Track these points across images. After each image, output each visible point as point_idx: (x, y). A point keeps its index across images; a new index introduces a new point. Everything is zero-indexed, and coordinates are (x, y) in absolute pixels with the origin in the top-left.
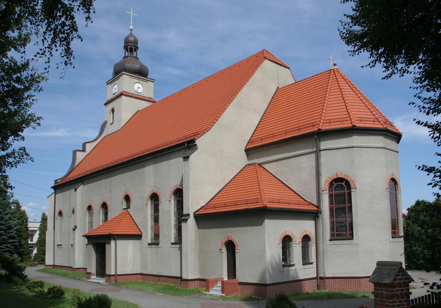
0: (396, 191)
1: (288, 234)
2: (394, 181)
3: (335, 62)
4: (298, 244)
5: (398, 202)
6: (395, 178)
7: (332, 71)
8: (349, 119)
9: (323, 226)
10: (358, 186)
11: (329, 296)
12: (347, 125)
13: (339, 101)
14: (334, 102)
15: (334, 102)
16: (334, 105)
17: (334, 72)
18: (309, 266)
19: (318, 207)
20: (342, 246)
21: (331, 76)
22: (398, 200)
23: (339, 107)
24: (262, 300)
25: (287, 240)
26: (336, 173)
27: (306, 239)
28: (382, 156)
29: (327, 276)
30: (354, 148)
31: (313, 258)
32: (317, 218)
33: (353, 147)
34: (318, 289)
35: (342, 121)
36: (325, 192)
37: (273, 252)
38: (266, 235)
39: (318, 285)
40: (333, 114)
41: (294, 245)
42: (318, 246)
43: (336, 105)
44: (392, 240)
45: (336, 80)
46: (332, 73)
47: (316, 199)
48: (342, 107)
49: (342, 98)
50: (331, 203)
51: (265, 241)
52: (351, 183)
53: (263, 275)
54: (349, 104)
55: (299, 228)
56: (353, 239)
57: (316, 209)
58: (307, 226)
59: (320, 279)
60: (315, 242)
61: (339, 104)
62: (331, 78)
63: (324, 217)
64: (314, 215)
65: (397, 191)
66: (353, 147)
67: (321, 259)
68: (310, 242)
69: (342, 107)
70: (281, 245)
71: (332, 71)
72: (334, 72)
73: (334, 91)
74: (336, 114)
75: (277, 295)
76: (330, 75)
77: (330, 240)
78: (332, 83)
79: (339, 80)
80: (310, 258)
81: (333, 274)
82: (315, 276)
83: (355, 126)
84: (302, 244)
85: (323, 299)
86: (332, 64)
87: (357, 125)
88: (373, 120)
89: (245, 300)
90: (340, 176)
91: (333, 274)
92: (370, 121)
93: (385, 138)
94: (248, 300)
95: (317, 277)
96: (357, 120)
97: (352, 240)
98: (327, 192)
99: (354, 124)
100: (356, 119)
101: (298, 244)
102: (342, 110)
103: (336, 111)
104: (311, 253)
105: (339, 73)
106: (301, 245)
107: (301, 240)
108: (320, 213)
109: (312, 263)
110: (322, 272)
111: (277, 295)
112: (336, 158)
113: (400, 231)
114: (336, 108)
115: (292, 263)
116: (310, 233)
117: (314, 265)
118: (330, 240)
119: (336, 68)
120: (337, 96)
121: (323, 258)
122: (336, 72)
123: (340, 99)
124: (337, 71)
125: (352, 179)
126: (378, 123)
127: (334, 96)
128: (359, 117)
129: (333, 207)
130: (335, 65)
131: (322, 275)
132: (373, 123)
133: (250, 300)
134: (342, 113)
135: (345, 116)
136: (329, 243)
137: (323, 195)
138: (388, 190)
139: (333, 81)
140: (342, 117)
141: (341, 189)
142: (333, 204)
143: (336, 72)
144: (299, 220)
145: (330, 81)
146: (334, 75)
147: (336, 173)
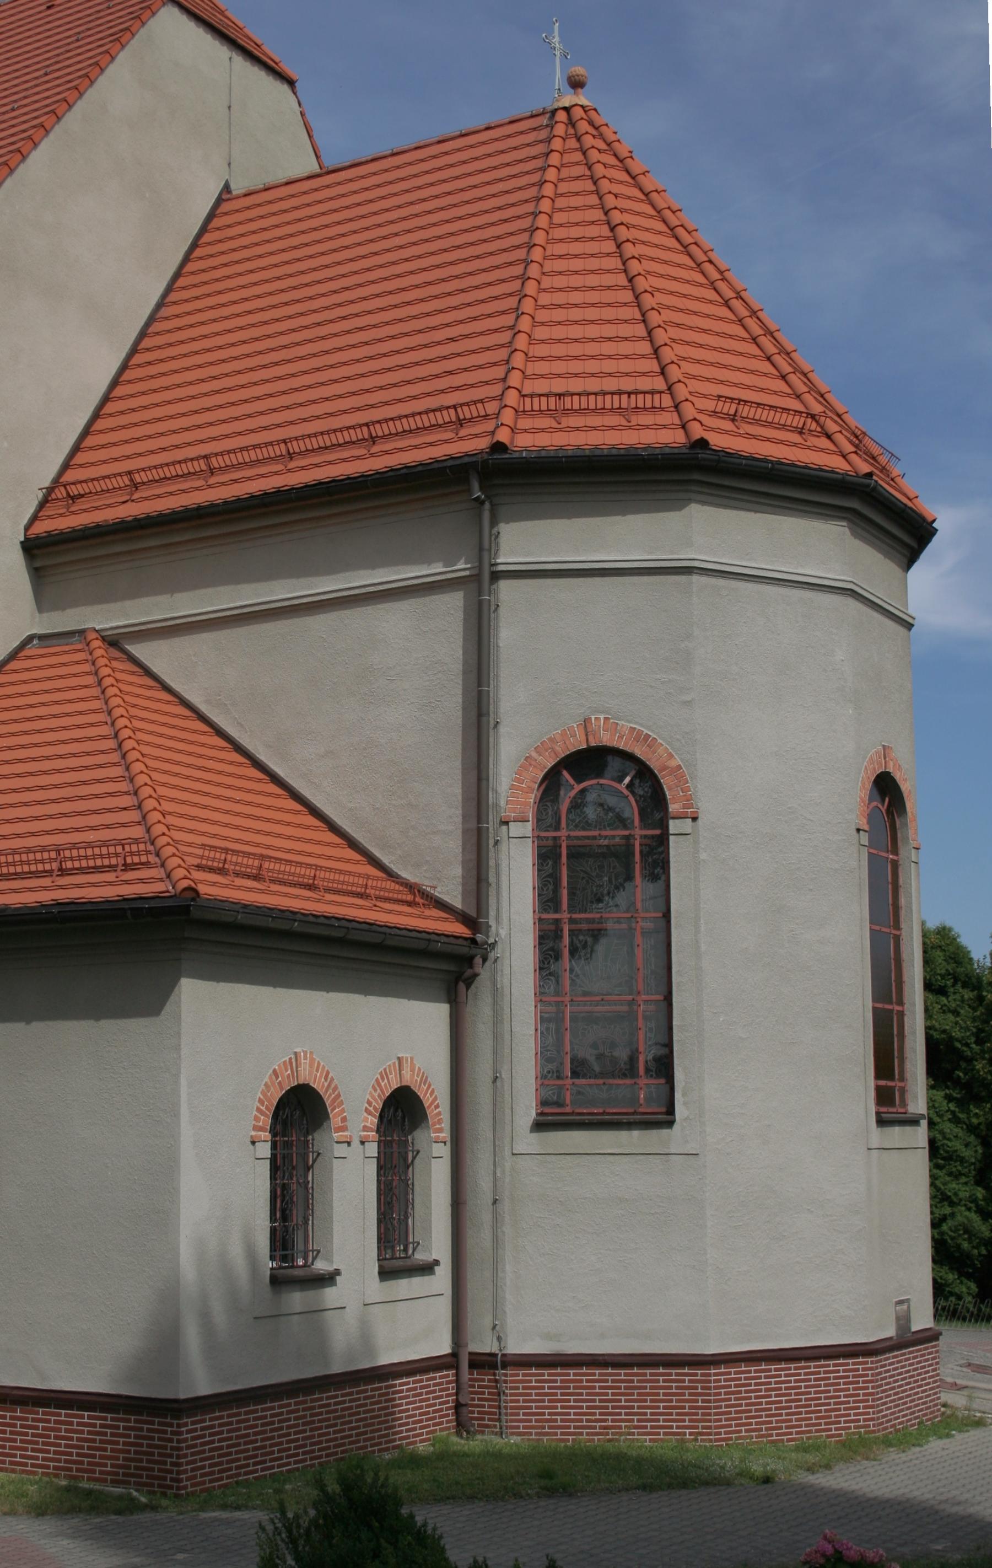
0: (895, 851)
1: (305, 1076)
2: (886, 788)
3: (579, 70)
4: (356, 1142)
5: (903, 913)
6: (897, 776)
7: (562, 116)
8: (667, 401)
9: (497, 1037)
10: (706, 805)
11: (547, 1474)
12: (661, 435)
13: (608, 296)
14: (576, 297)
15: (576, 297)
16: (576, 314)
17: (572, 123)
18: (415, 1285)
19: (473, 922)
20: (608, 1165)
21: (557, 144)
22: (903, 901)
23: (609, 330)
24: (153, 1508)
25: (299, 1113)
26: (587, 721)
27: (401, 1111)
28: (839, 637)
29: (515, 1347)
30: (695, 578)
31: (436, 1243)
32: (462, 986)
33: (688, 570)
34: (461, 1426)
35: (627, 404)
36: (516, 829)
37: (217, 1195)
38: (183, 1081)
39: (458, 1406)
40: (576, 367)
41: (340, 1150)
42: (468, 1157)
43: (592, 314)
44: (877, 1136)
45: (581, 170)
46: (560, 129)
47: (458, 871)
48: (625, 330)
49: (622, 280)
50: (547, 898)
51: (176, 1115)
52: (667, 782)
53: (164, 1344)
54: (667, 315)
55: (371, 1041)
56: (670, 1124)
57: (459, 929)
58: (398, 1036)
59: (475, 1368)
60: (446, 1135)
61: (609, 313)
62: (554, 159)
63: (503, 981)
64: (447, 964)
65: (902, 852)
66: (688, 570)
67: (479, 1239)
68: (420, 1138)
69: (625, 330)
70: (265, 1150)
71: (562, 116)
72: (572, 123)
73: (575, 232)
74: (592, 366)
75: (320, 1484)
76: (549, 140)
77: (540, 1126)
78: (563, 188)
79: (599, 170)
80: (416, 1234)
81: (548, 1337)
82: (443, 1347)
83: (702, 443)
84: (274, 1146)
85: (517, 1496)
86: (559, 79)
87: (717, 441)
88: (798, 421)
89: (40, 1511)
90: (606, 739)
91: (548, 1337)
92: (783, 427)
93: (855, 534)
94: (76, 1502)
95: (454, 1355)
96: (714, 414)
97: (665, 1132)
98: (527, 829)
99: (697, 432)
100: (710, 405)
101: (356, 1142)
102: (625, 348)
103: (592, 349)
104: (428, 1206)
105: (601, 136)
106: (372, 1149)
107: (373, 1121)
108: (485, 960)
109: (428, 1268)
110: (487, 1322)
111: (320, 1484)
112: (612, 629)
113: (910, 1086)
114: (593, 331)
115: (321, 1266)
116: (424, 1080)
117: (442, 1279)
118: (540, 1126)
119: (583, 101)
120: (593, 264)
121: (496, 1241)
122: (583, 126)
123: (609, 280)
124: (591, 123)
125: (677, 761)
126: (824, 443)
127: (577, 264)
128: (716, 404)
129: (557, 921)
130: (576, 84)
131: (486, 1345)
132: (796, 438)
133: (73, 1510)
134: (626, 366)
135: (644, 384)
136: (528, 1141)
137: (503, 847)
138: (865, 839)
139: (565, 173)
140: (627, 384)
141: (612, 822)
142: (557, 910)
143: (583, 126)
144: (366, 991)
145: (551, 174)
146: (572, 143)
147: (587, 721)
